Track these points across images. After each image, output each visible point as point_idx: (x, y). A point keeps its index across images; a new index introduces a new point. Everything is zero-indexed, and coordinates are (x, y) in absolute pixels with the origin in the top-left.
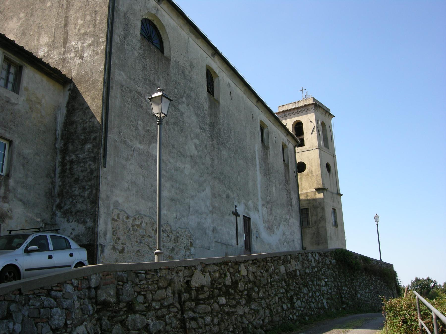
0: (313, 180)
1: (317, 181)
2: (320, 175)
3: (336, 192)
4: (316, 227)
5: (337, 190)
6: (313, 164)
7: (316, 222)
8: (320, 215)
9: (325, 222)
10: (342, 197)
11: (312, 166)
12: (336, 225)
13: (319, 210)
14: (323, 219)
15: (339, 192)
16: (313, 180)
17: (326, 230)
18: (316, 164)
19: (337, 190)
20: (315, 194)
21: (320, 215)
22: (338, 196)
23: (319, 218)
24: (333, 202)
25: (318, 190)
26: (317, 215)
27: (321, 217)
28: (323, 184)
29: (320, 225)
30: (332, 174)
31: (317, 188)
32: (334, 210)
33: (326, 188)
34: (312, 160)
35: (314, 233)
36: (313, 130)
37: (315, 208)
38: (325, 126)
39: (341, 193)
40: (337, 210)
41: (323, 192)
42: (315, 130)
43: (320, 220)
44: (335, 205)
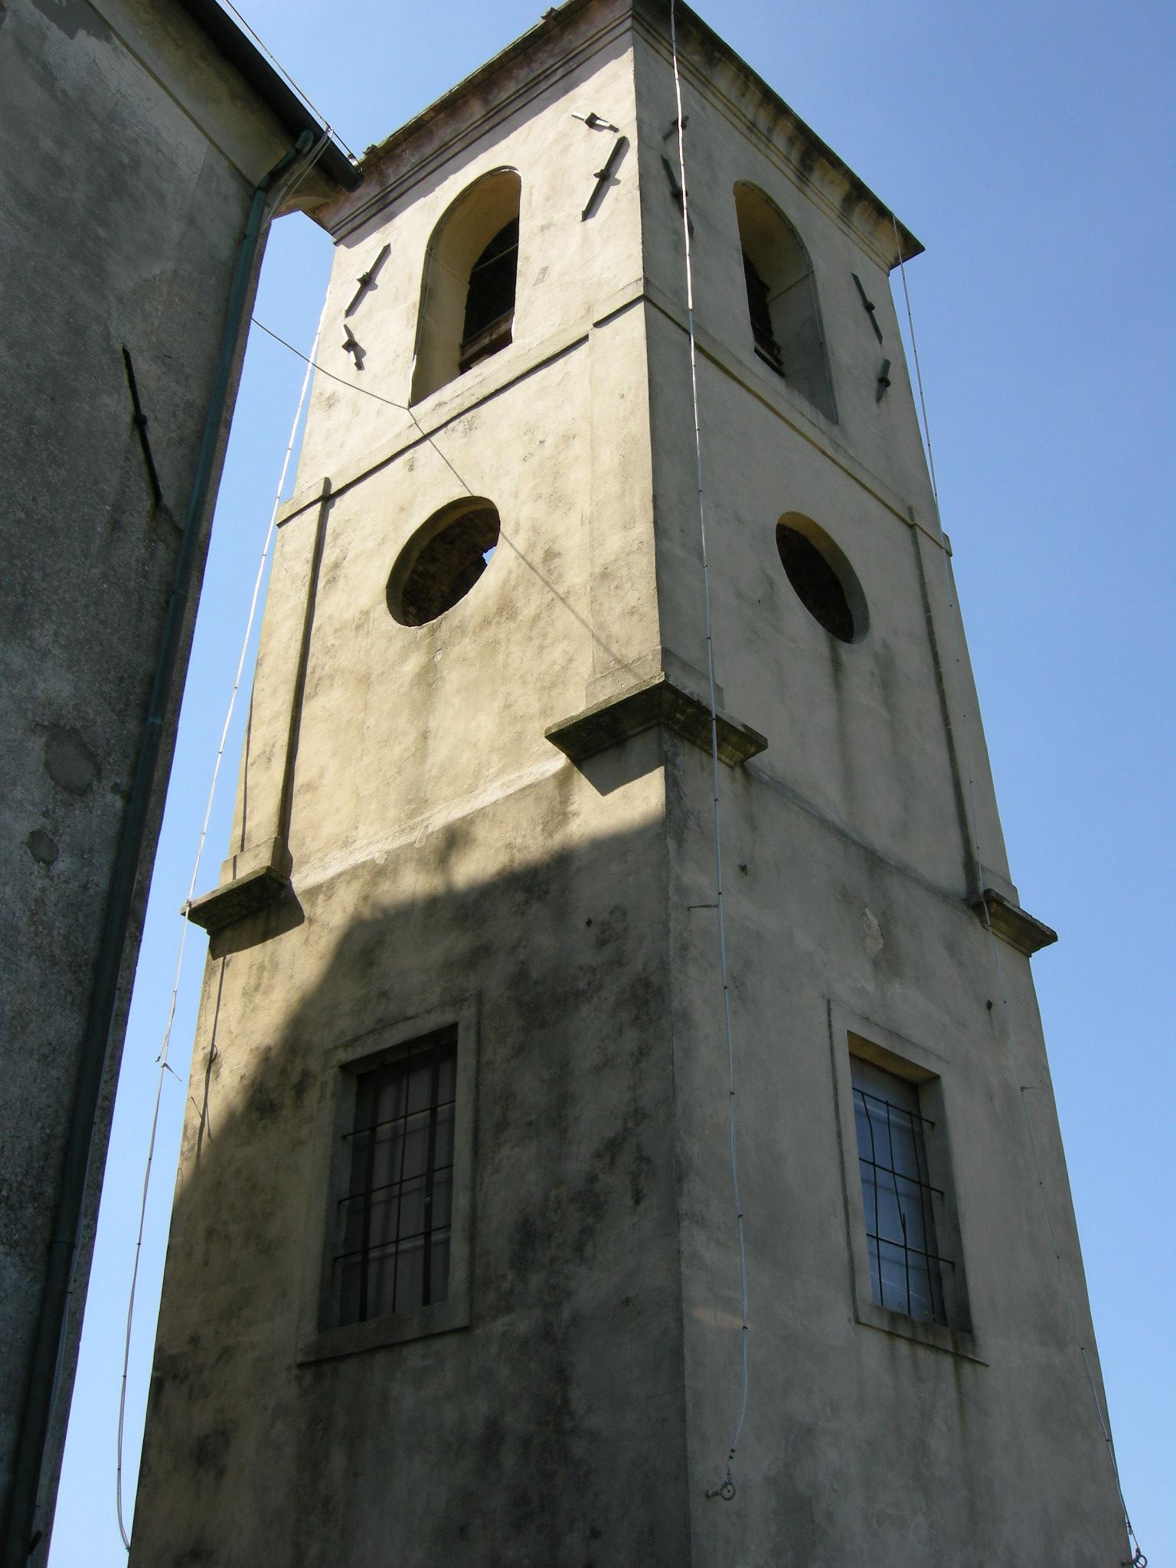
0: (556, 654)
1: (603, 642)
2: (646, 562)
3: (949, 874)
4: (524, 1323)
5: (970, 867)
6: (577, 478)
7: (529, 1234)
8: (596, 1111)
9: (673, 1219)
10: (1040, 959)
11: (557, 501)
12: (937, 1311)
13: (590, 1030)
14: (645, 1163)
15: (984, 883)
16: (556, 654)
17: (672, 1355)
18: (608, 459)
19: (970, 867)
20: (560, 813)
21: (596, 1111)
22: (992, 949)
23: (578, 1163)
24: (888, 962)
25: (596, 742)
26: (557, 1117)
27: (612, 1148)
28: (667, 655)
29: (590, 1288)
30: (887, 682)
31: (576, 704)
32: (902, 1094)
33: (737, 705)
34: (569, 438)
35: (493, 1435)
36: (605, 178)
37: (542, 1003)
38: (800, 247)
39: (1032, 903)
40: (965, 1114)
41: (665, 760)
42: (629, 168)
43: (592, 1201)
44: (923, 1022)
